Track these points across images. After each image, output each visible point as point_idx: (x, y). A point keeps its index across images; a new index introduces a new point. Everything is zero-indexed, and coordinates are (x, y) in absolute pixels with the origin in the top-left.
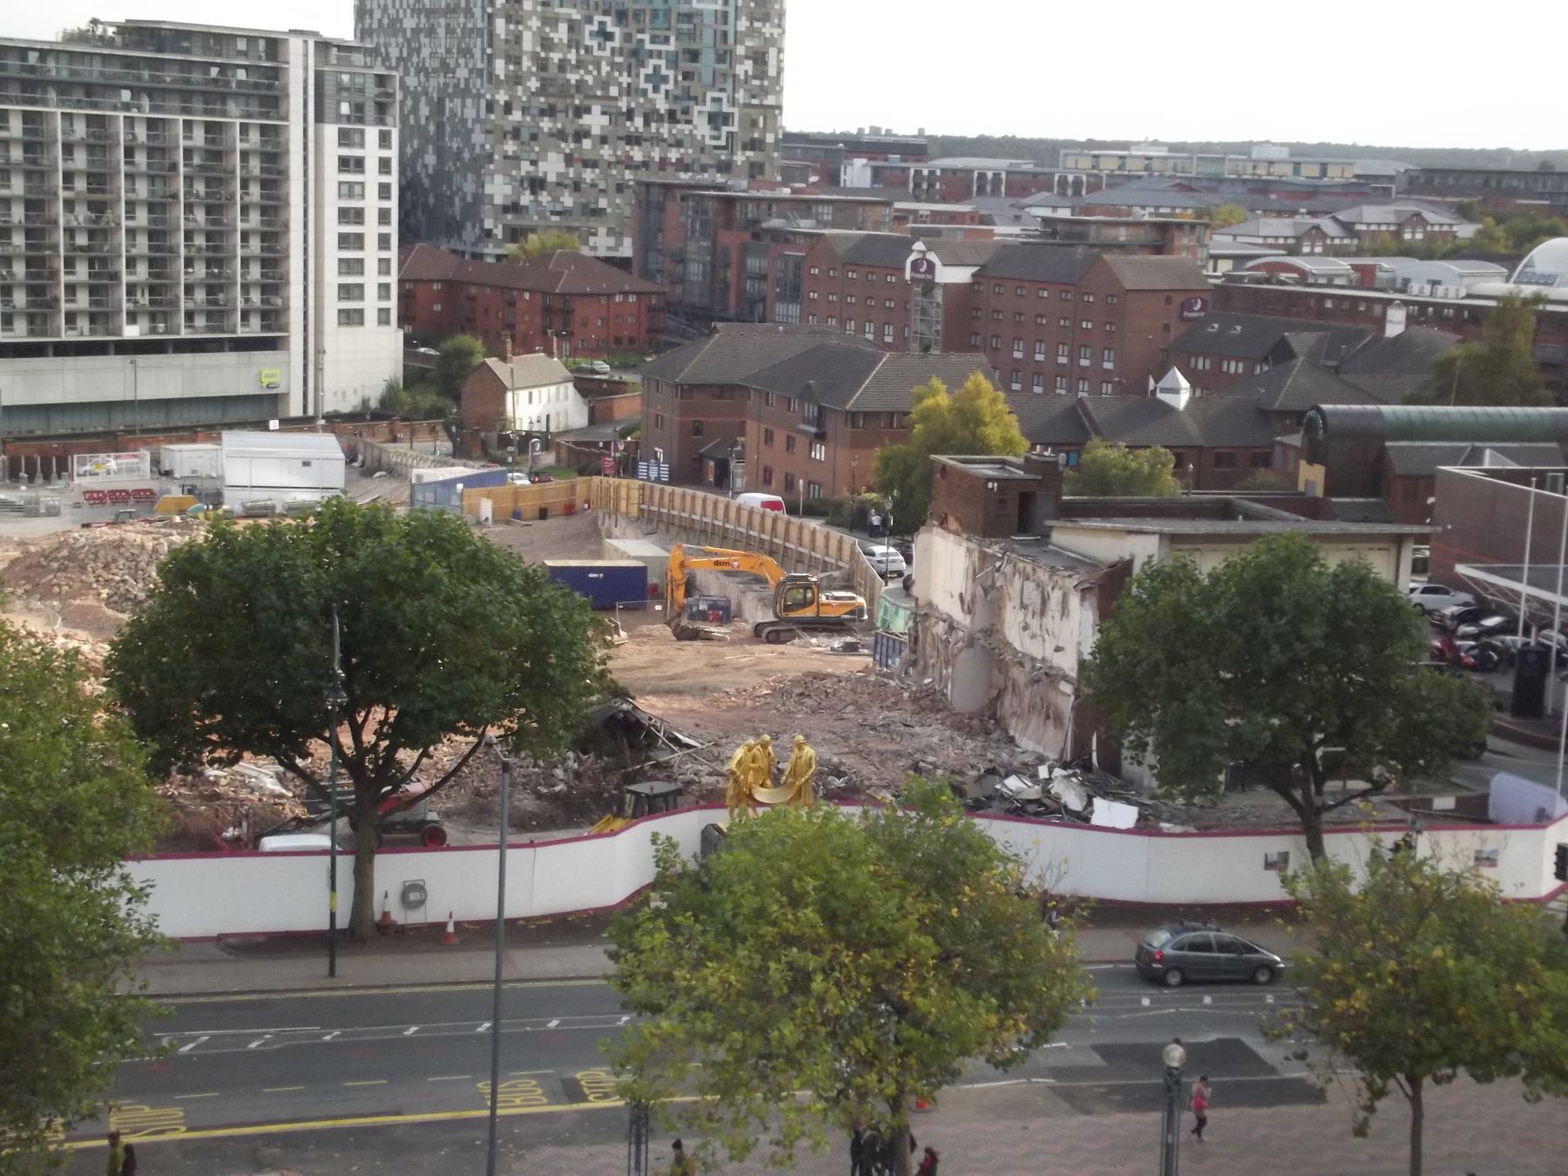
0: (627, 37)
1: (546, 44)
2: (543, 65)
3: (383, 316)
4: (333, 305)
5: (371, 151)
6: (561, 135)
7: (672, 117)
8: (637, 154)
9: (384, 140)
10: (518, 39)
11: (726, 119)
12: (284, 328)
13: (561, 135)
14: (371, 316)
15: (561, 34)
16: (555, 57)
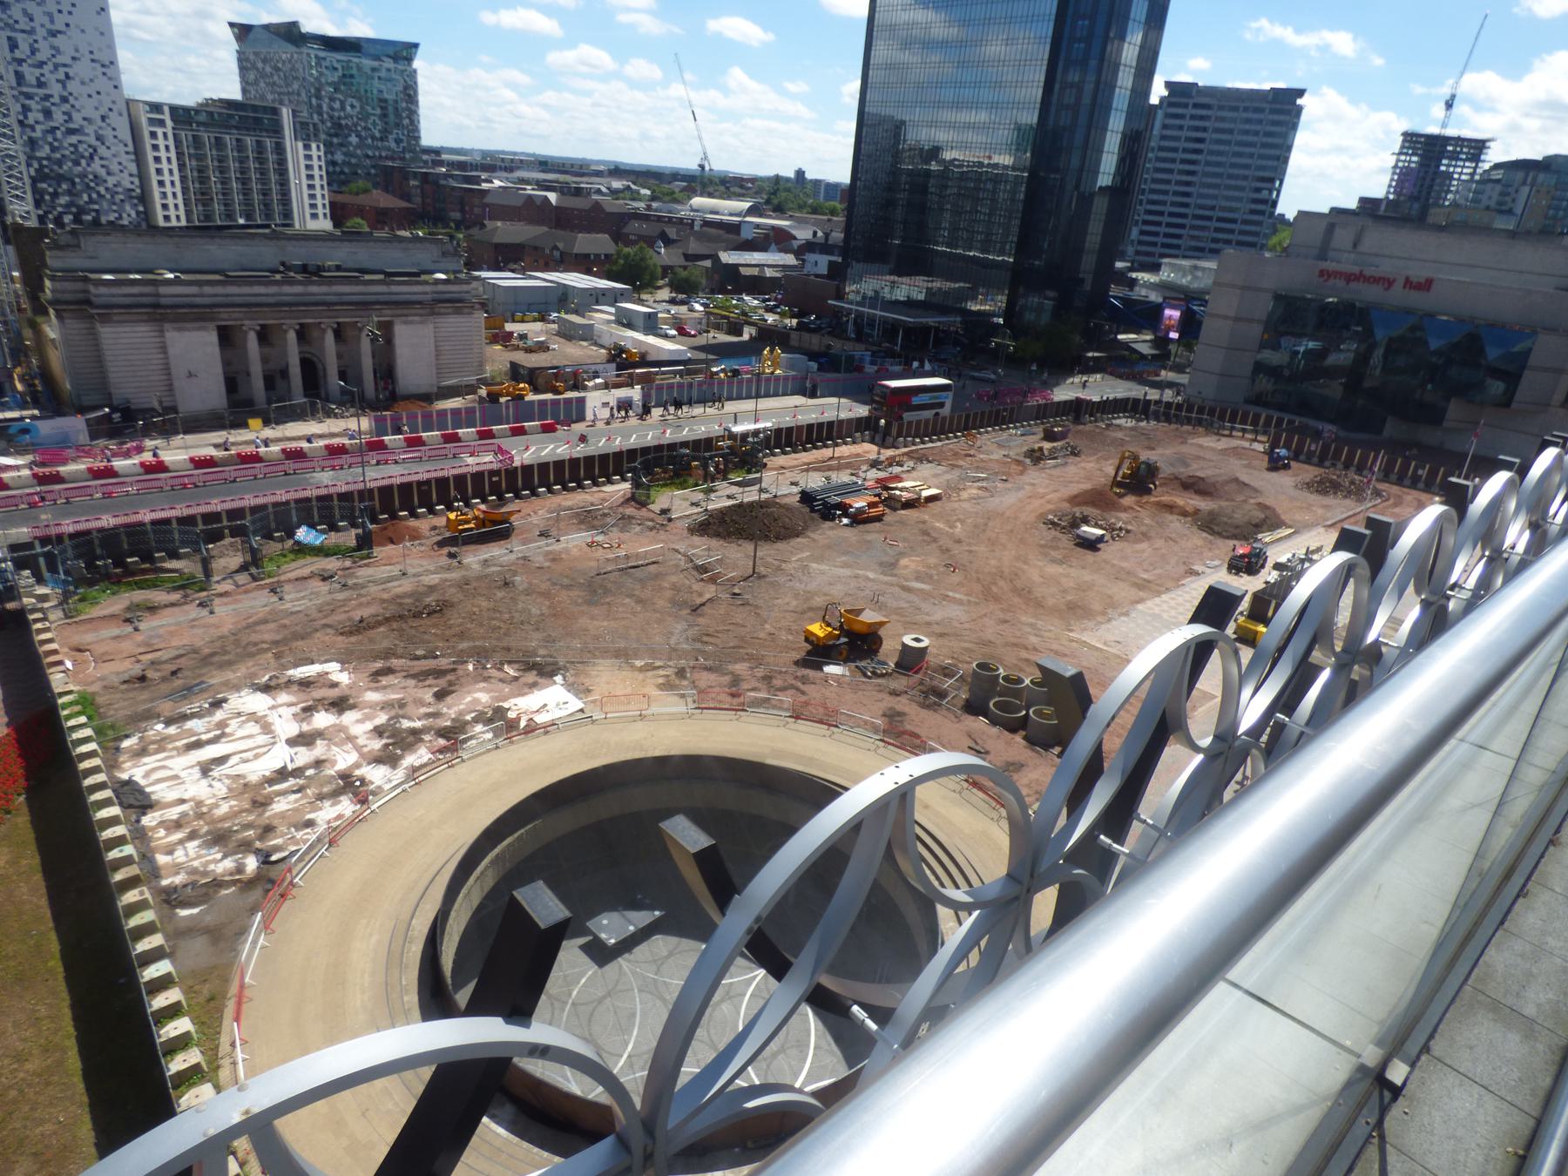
0: (362, 108)
1: (332, 109)
2: (332, 117)
3: (325, 214)
4: (308, 211)
5: (314, 152)
6: (341, 145)
7: (382, 139)
8: (370, 153)
9: (318, 147)
10: (320, 106)
11: (401, 141)
12: (292, 219)
13: (341, 145)
14: (321, 216)
15: (337, 105)
16: (336, 114)
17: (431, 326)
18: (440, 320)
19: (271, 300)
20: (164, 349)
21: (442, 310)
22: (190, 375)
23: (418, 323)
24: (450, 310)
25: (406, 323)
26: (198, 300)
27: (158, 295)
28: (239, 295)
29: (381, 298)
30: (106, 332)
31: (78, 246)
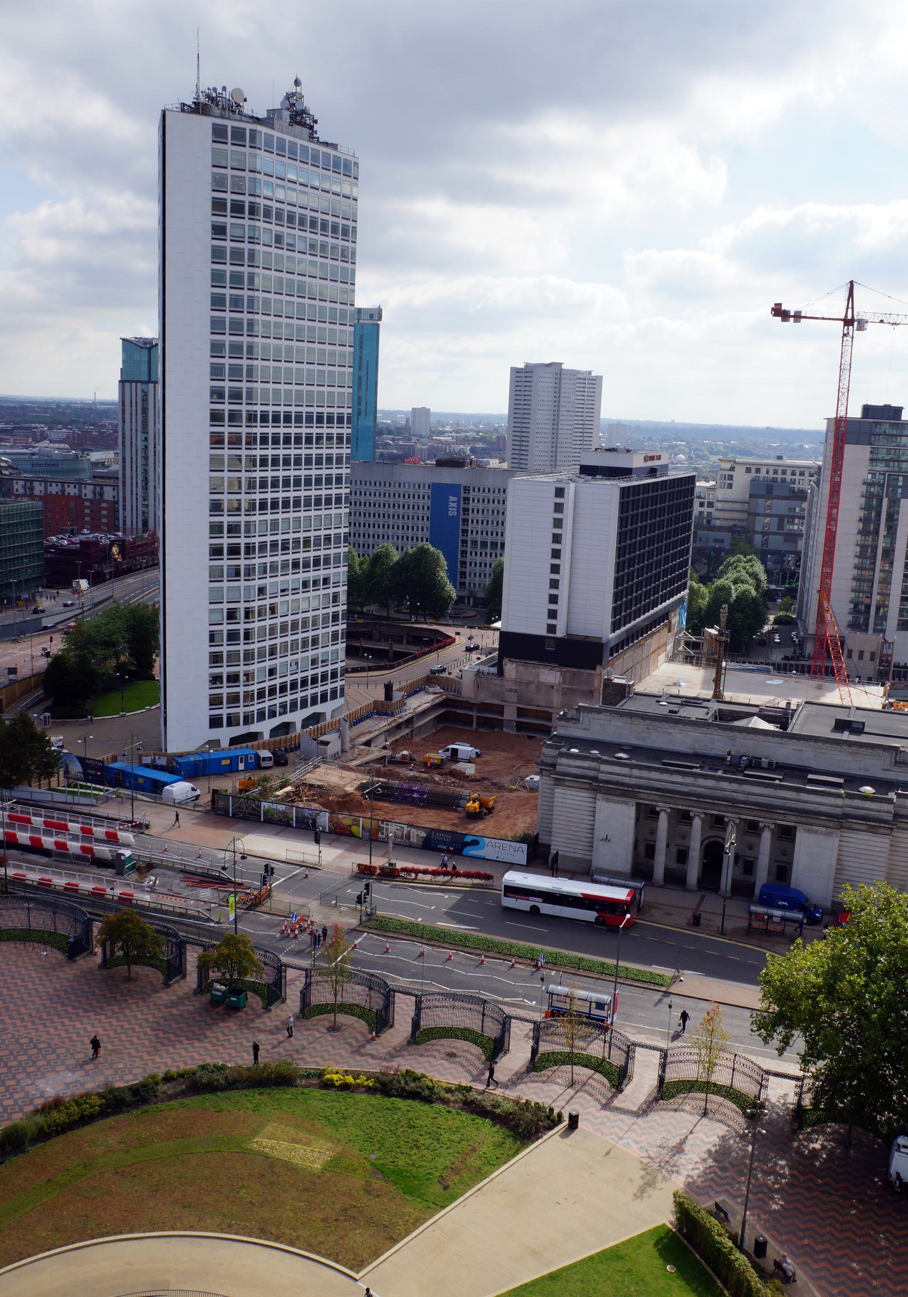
17: (836, 840)
18: (847, 834)
19: (685, 789)
20: (594, 812)
21: (855, 826)
22: (607, 839)
23: (821, 833)
24: (863, 827)
25: (809, 831)
26: (627, 780)
27: (598, 770)
28: (660, 781)
29: (788, 804)
30: (559, 791)
31: (578, 720)
